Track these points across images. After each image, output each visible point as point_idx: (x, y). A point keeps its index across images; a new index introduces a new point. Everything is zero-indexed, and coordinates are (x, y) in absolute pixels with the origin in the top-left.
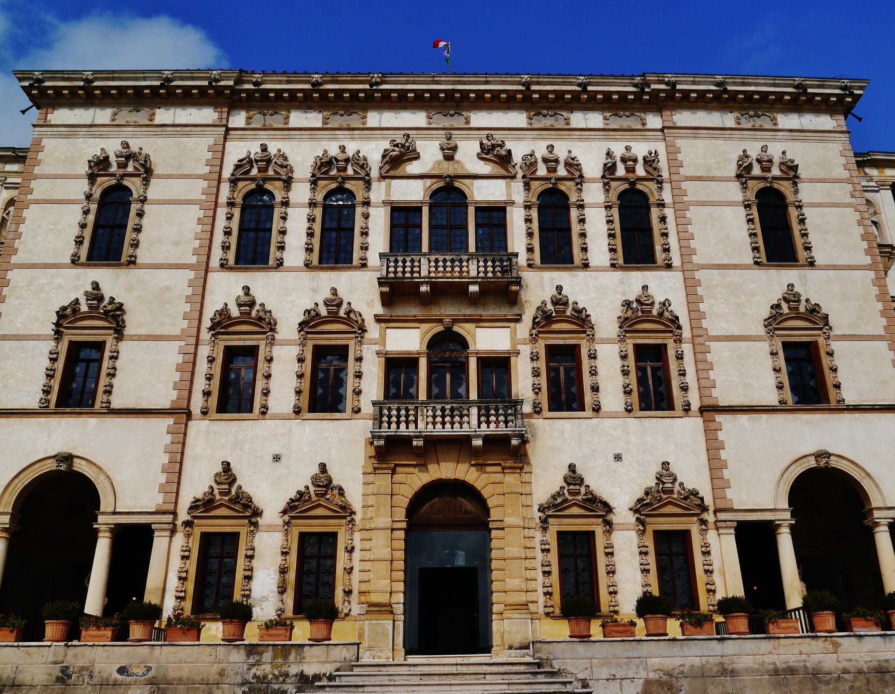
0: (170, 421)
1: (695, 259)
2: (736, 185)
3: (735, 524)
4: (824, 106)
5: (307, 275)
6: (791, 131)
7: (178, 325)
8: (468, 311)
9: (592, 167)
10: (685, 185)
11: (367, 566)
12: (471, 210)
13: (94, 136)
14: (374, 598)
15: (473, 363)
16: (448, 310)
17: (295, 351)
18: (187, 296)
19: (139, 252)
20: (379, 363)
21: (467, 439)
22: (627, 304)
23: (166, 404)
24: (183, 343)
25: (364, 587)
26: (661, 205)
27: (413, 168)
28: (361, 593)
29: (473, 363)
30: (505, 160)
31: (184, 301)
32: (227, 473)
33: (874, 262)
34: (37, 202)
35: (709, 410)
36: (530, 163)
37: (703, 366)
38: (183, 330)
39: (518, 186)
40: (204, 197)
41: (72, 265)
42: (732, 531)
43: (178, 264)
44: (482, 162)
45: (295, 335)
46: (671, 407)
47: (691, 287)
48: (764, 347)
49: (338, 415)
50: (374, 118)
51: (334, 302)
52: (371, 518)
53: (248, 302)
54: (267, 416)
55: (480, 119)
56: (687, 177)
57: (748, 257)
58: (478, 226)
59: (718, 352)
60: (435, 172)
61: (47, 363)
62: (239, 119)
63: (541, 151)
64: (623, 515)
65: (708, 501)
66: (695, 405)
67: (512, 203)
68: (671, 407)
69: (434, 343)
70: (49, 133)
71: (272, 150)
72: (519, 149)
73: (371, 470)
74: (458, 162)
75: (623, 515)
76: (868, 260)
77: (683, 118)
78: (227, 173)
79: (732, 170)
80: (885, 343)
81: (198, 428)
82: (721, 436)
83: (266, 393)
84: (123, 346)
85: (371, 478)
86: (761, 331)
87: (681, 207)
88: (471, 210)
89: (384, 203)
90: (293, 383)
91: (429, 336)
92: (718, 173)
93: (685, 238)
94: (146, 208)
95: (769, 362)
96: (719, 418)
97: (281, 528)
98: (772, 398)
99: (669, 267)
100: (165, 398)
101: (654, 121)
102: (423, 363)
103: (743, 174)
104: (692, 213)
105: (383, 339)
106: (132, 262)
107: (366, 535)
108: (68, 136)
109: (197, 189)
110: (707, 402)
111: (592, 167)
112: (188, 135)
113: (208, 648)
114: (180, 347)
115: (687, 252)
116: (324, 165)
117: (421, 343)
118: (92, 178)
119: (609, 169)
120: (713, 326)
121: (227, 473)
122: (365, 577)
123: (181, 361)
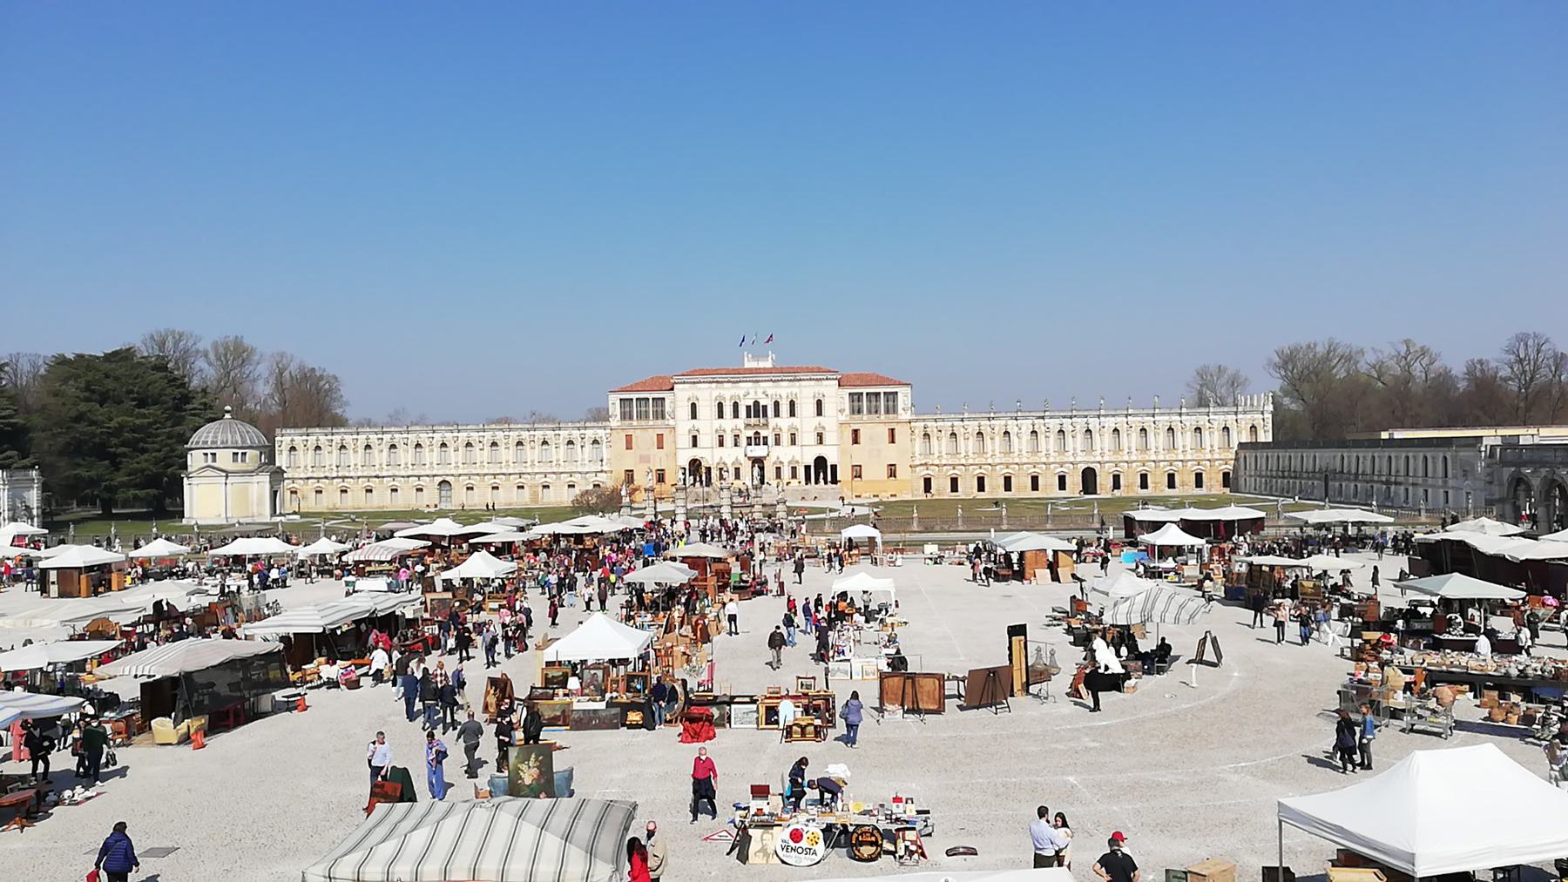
4: (833, 379)
7: (709, 432)
9: (784, 396)
27: (748, 397)
30: (767, 395)
36: (772, 395)
50: (741, 384)
55: (762, 384)
59: (805, 435)
64: (786, 464)
72: (769, 393)
75: (786, 464)
77: (803, 383)
78: (714, 398)
79: (812, 395)
81: (715, 449)
87: (801, 404)
93: (801, 411)
98: (813, 443)
100: (710, 446)
101: (797, 383)
103: (814, 396)
104: (803, 406)
109: (708, 403)
111: (784, 396)
119: (787, 397)
120: (804, 430)
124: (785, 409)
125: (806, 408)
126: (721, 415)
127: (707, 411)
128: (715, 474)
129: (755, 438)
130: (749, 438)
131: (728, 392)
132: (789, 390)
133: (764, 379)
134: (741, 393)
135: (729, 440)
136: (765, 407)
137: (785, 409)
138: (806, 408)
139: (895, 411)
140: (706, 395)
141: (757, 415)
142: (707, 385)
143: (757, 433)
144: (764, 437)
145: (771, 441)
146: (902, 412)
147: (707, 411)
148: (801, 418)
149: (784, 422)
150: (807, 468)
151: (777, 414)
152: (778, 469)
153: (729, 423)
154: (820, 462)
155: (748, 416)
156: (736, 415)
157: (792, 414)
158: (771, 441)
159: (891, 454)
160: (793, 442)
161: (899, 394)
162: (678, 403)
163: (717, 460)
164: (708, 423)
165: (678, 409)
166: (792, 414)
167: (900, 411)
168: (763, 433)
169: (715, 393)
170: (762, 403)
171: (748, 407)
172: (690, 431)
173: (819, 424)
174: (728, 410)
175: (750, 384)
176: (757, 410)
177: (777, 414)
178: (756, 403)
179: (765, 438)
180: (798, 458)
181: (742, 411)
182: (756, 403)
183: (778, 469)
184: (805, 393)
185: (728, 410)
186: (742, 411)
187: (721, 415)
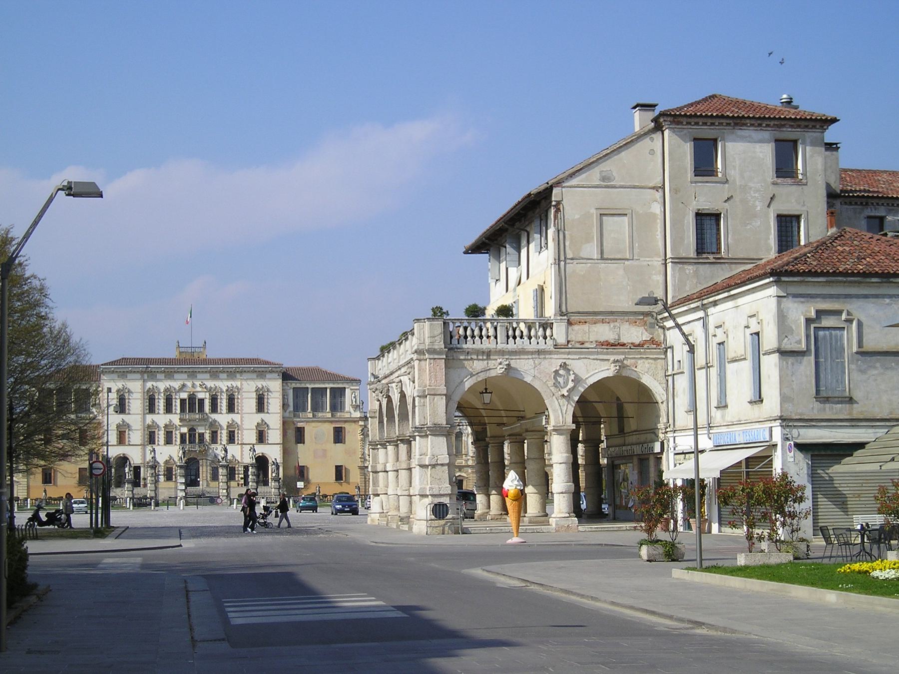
0: (141, 447)
1: (243, 412)
2: (255, 394)
5: (164, 415)
8: (196, 423)
10: (243, 394)
12: (197, 400)
15: (197, 434)
16: (192, 423)
17: (163, 432)
21: (196, 451)
22: (228, 422)
23: (139, 444)
26: (238, 398)
27: (184, 389)
29: (197, 434)
37: (242, 435)
39: (208, 394)
45: (163, 429)
46: (234, 443)
48: (255, 431)
51: (171, 421)
55: (199, 376)
57: (255, 411)
58: (198, 403)
62: (146, 376)
63: (213, 386)
65: (240, 461)
66: (240, 443)
67: (206, 398)
69: (190, 430)
79: (254, 389)
86: (255, 428)
87: (242, 399)
88: (197, 400)
90: (163, 439)
92: (251, 390)
94: (130, 401)
95: (255, 435)
99: (238, 413)
102: (187, 434)
105: (180, 429)
106: (129, 414)
109: (139, 396)
115: (242, 410)
116: (166, 390)
118: (117, 394)
119: (227, 390)
124: (223, 404)
125: (248, 403)
126: (151, 408)
127: (136, 404)
129: (190, 436)
130: (183, 436)
131: (162, 385)
132: (229, 383)
133: (199, 370)
134: (176, 385)
135: (161, 436)
136: (201, 401)
137: (223, 404)
138: (248, 403)
139: (342, 408)
140: (136, 387)
141: (192, 410)
142: (138, 376)
144: (199, 434)
145: (207, 437)
146: (352, 410)
147: (136, 404)
148: (242, 414)
149: (223, 418)
150: (246, 468)
151: (214, 409)
153: (161, 419)
154: (262, 462)
155: (183, 410)
156: (169, 409)
157: (231, 408)
158: (207, 437)
159: (338, 454)
161: (346, 390)
164: (135, 416)
166: (231, 408)
167: (348, 406)
170: (200, 396)
171: (183, 401)
173: (263, 420)
174: (161, 404)
175: (185, 376)
176: (192, 404)
177: (214, 409)
178: (192, 397)
179: (202, 436)
180: (239, 458)
181: (177, 405)
182: (192, 397)
184: (248, 388)
185: (161, 404)
186: (177, 405)
187: (151, 408)
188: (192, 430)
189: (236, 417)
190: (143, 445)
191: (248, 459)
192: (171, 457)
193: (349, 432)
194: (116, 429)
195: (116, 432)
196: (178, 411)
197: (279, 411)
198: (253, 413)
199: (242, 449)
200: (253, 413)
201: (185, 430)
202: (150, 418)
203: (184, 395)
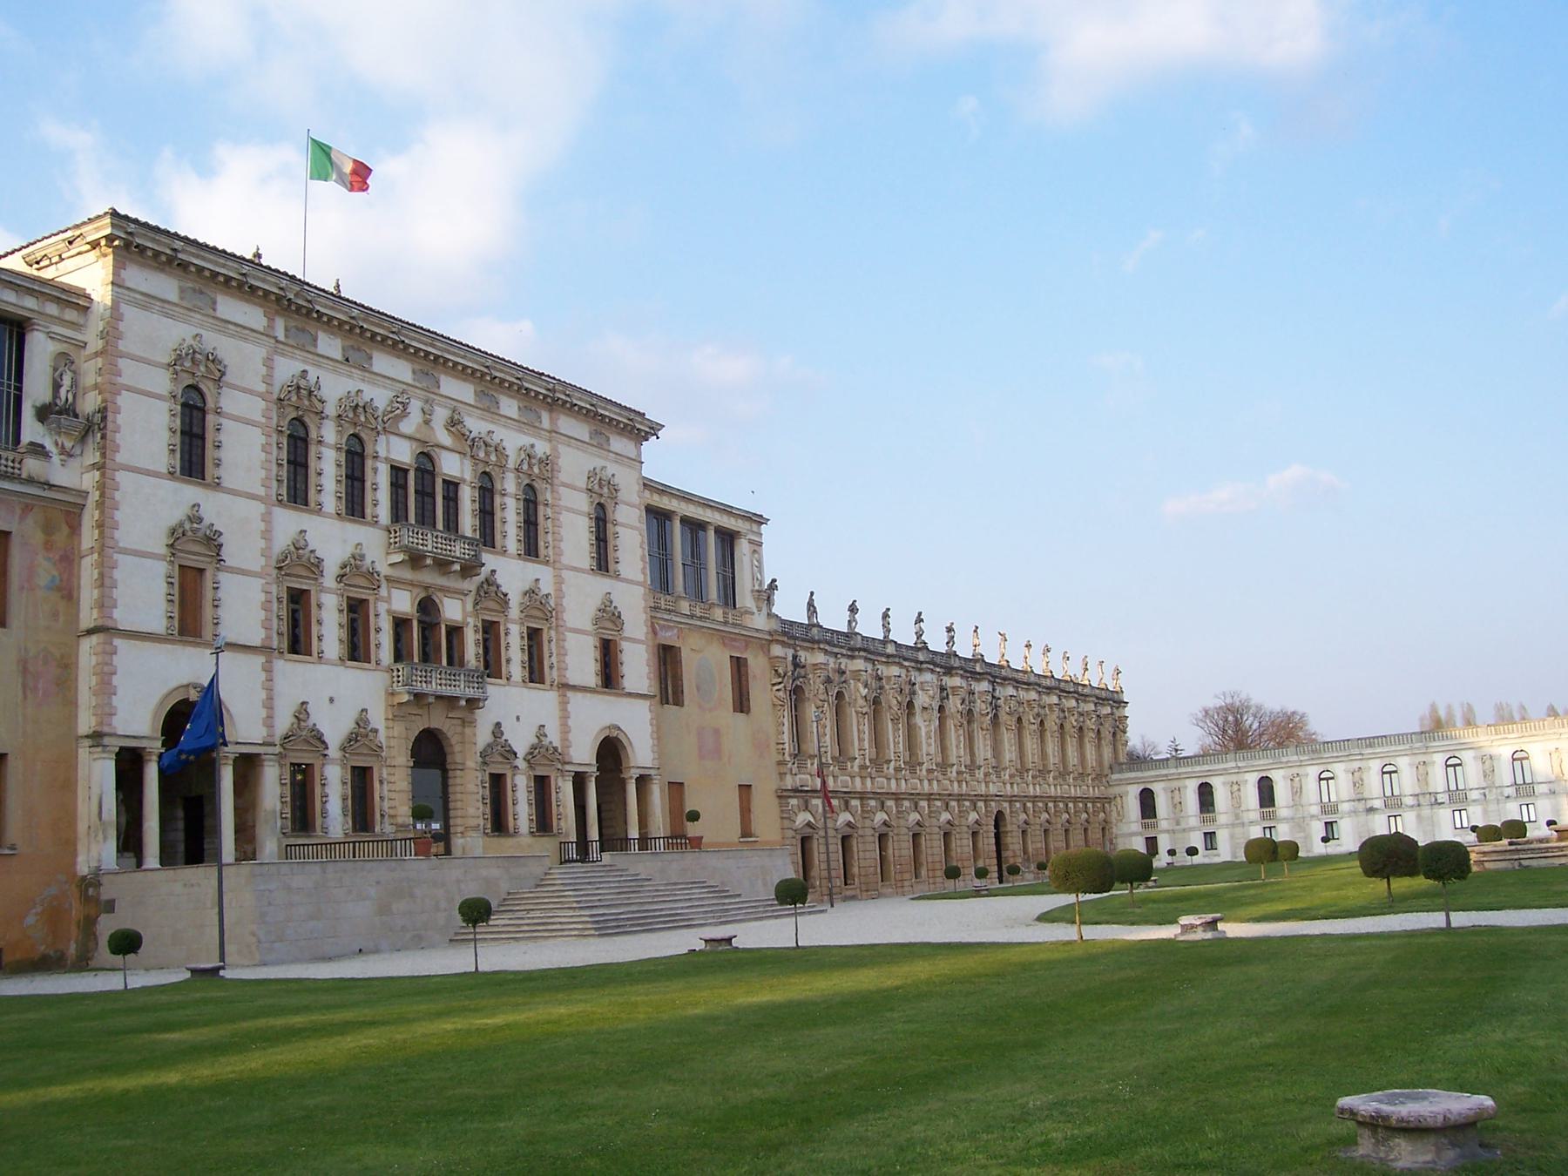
3: (573, 774)
5: (337, 524)
6: (617, 454)
7: (256, 564)
11: (393, 795)
13: (167, 315)
14: (400, 820)
18: (262, 531)
19: (222, 472)
20: (389, 619)
23: (257, 642)
24: (264, 581)
25: (392, 812)
28: (390, 816)
31: (259, 536)
32: (302, 712)
33: (645, 581)
34: (129, 389)
35: (565, 687)
38: (262, 567)
40: (263, 420)
41: (170, 476)
42: (571, 778)
43: (253, 494)
44: (446, 432)
47: (559, 581)
49: (366, 665)
52: (394, 757)
53: (298, 546)
54: (323, 661)
56: (562, 483)
60: (418, 436)
61: (164, 588)
68: (542, 682)
70: (127, 298)
71: (312, 376)
73: (390, 717)
74: (432, 428)
76: (640, 578)
80: (645, 646)
82: (569, 707)
83: (320, 639)
84: (223, 577)
85: (391, 724)
86: (589, 627)
89: (386, 459)
91: (417, 603)
96: (570, 694)
97: (339, 762)
105: (388, 600)
107: (391, 770)
108: (145, 308)
109: (254, 408)
110: (564, 681)
112: (246, 339)
113: (471, 860)
114: (263, 585)
115: (559, 553)
117: (412, 605)
121: (302, 712)
122: (393, 803)
123: (263, 599)
126: (297, 491)
128: (272, 788)
130: (400, 624)
141: (426, 519)
143: (427, 607)
152: (497, 782)
160: (535, 674)
162: (130, 372)
163: (283, 723)
165: (124, 400)
168: (452, 610)
169: (288, 368)
170: (451, 465)
172: (177, 536)
174: (328, 467)
182: (426, 463)
183: (497, 782)
185: (328, 467)
187: (297, 491)
188: (427, 607)
189: (543, 575)
190: (218, 651)
191: (583, 753)
192: (362, 721)
193: (755, 676)
194: (164, 551)
195: (162, 568)
196: (384, 512)
197: (640, 578)
198: (582, 571)
199: (564, 704)
200: (582, 571)
201: (404, 602)
202: (289, 523)
203: (404, 453)
